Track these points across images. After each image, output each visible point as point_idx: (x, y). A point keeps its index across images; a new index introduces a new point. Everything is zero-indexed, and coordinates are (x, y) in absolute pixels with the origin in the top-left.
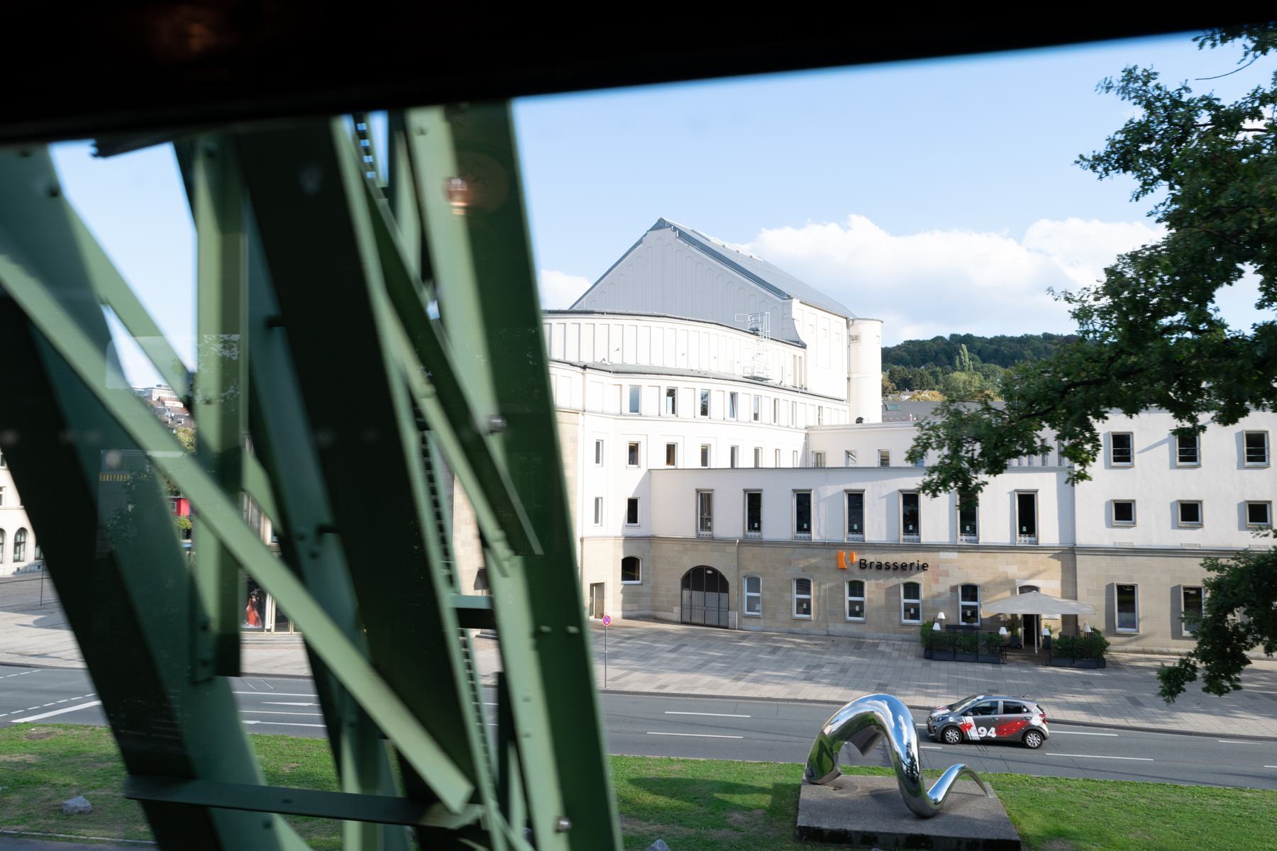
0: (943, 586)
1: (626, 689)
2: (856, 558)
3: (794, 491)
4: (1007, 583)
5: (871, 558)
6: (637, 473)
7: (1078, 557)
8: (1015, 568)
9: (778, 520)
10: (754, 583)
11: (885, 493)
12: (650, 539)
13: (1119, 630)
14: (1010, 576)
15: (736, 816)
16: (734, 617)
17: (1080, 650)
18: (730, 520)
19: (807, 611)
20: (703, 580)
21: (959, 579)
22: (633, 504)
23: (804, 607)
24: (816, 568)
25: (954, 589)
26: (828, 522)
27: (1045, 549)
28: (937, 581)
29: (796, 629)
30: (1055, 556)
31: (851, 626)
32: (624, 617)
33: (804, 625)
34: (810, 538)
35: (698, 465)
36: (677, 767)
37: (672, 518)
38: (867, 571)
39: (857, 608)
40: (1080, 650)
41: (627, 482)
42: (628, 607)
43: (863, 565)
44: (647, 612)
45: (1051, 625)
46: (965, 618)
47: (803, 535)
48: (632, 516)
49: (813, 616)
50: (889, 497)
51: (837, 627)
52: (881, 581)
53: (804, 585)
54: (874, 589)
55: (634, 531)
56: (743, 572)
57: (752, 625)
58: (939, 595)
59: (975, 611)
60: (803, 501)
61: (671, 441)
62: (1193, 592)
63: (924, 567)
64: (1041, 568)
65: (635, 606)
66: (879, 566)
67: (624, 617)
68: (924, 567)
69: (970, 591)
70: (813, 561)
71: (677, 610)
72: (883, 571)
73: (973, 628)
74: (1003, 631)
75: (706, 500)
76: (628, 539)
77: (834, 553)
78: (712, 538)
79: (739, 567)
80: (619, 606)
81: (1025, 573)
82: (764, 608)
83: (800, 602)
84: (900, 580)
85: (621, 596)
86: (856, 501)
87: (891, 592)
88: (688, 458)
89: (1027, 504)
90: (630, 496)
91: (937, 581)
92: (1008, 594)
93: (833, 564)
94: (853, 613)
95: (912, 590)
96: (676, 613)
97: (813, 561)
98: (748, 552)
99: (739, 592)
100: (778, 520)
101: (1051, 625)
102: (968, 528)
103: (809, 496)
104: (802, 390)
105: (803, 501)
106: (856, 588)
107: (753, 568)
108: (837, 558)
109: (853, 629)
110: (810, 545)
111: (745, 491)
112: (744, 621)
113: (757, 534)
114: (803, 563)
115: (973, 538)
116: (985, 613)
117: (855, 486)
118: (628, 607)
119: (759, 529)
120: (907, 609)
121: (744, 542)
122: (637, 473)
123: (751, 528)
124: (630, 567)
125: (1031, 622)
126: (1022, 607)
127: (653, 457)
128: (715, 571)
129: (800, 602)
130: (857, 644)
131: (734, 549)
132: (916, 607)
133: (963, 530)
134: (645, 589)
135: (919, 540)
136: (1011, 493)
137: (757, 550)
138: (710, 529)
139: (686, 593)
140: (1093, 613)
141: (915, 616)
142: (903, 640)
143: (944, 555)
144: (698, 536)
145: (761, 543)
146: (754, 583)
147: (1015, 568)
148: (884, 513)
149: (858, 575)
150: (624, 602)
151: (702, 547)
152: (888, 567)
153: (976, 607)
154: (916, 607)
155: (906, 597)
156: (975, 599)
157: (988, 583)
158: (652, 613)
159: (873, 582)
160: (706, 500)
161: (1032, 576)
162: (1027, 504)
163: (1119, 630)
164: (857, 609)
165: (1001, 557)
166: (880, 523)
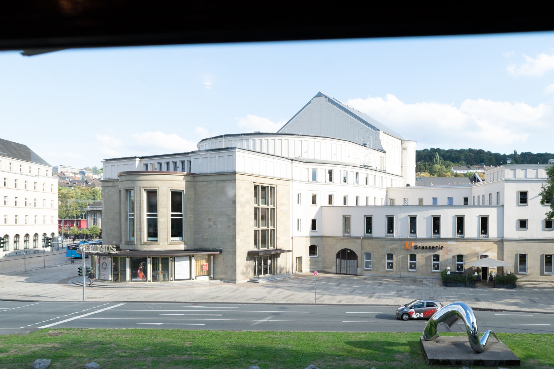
0: (449, 256)
1: (325, 303)
2: (413, 244)
3: (387, 216)
4: (476, 254)
5: (419, 244)
6: (315, 208)
8: (479, 248)
9: (380, 228)
10: (369, 256)
11: (426, 217)
12: (322, 237)
13: (519, 272)
14: (477, 251)
15: (398, 356)
16: (360, 270)
17: (506, 281)
18: (358, 228)
19: (392, 267)
20: (346, 255)
22: (314, 222)
23: (390, 266)
24: (396, 249)
25: (454, 257)
26: (401, 229)
28: (447, 254)
29: (386, 275)
30: (495, 243)
31: (411, 273)
32: (311, 272)
33: (390, 273)
34: (393, 236)
35: (342, 204)
36: (363, 336)
37: (332, 228)
38: (417, 250)
39: (413, 266)
40: (506, 281)
41: (312, 212)
42: (312, 267)
43: (416, 247)
44: (321, 269)
45: (493, 271)
46: (458, 269)
47: (390, 235)
48: (314, 227)
49: (394, 269)
50: (427, 218)
52: (424, 254)
53: (390, 256)
54: (420, 258)
55: (315, 233)
56: (364, 251)
57: (368, 274)
58: (448, 260)
59: (462, 266)
60: (391, 220)
61: (331, 194)
62: (549, 257)
63: (442, 248)
64: (490, 248)
65: (315, 267)
66: (423, 248)
67: (311, 272)
68: (442, 248)
69: (460, 258)
70: (394, 246)
71: (334, 268)
72: (424, 250)
73: (461, 273)
74: (476, 274)
76: (312, 237)
77: (403, 242)
78: (350, 237)
79: (362, 249)
80: (309, 267)
81: (483, 250)
82: (373, 267)
83: (389, 264)
85: (309, 263)
86: (413, 220)
87: (428, 259)
88: (338, 201)
89: (484, 221)
90: (313, 218)
91: (447, 254)
92: (476, 259)
93: (403, 247)
94: (411, 268)
95: (437, 258)
96: (334, 269)
97: (394, 246)
98: (366, 242)
99: (362, 260)
100: (380, 228)
101: (493, 271)
102: (460, 231)
103: (393, 218)
104: (384, 172)
105: (391, 220)
106: (413, 257)
107: (368, 249)
108: (405, 245)
109: (412, 275)
110: (394, 239)
111: (365, 216)
112: (364, 272)
113: (370, 234)
114: (390, 247)
115: (462, 235)
116: (466, 267)
117: (413, 214)
118: (312, 267)
119: (371, 232)
120: (434, 266)
121: (364, 238)
122: (315, 208)
123: (367, 232)
124: (313, 250)
125: (485, 270)
126: (482, 264)
127: (323, 201)
128: (351, 251)
129: (389, 264)
130: (414, 281)
131: (360, 241)
132: (438, 265)
133: (458, 232)
134: (320, 259)
135: (440, 237)
136: (478, 217)
137: (370, 241)
138: (349, 232)
139: (338, 260)
140: (509, 266)
141: (438, 268)
142: (432, 279)
143: (450, 243)
144: (344, 236)
145: (372, 238)
146: (369, 256)
147: (479, 248)
148: (425, 225)
149: (413, 252)
150: (311, 265)
151: (346, 240)
152: (426, 248)
153: (462, 264)
154: (438, 265)
155: (458, 261)
156: (462, 261)
157: (467, 255)
158: (323, 269)
159: (420, 254)
160: (347, 220)
161: (486, 251)
162: (484, 221)
163: (519, 272)
164: (413, 266)
165: (474, 243)
166: (424, 229)
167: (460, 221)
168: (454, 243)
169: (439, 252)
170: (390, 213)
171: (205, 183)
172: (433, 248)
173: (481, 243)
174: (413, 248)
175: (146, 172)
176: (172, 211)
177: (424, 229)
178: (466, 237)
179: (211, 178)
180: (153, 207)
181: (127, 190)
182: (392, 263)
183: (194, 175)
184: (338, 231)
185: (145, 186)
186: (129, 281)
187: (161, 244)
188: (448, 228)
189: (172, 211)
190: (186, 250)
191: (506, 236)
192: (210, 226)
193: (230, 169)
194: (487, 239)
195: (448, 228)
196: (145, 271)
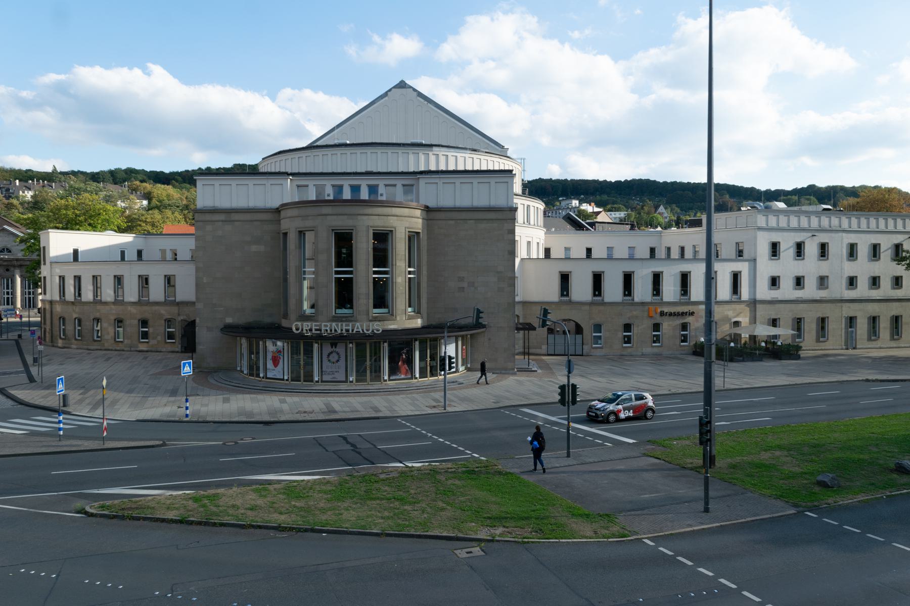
2: (659, 310)
5: (666, 310)
7: (758, 306)
18: (581, 290)
23: (628, 340)
26: (642, 290)
27: (744, 302)
29: (624, 353)
30: (748, 306)
43: (662, 314)
51: (648, 350)
53: (627, 327)
54: (668, 326)
57: (598, 353)
66: (671, 314)
70: (635, 313)
71: (544, 347)
75: (565, 278)
77: (646, 308)
78: (570, 302)
84: (679, 321)
93: (646, 314)
94: (654, 342)
95: (684, 327)
97: (635, 313)
100: (613, 290)
106: (657, 327)
109: (656, 350)
121: (591, 304)
129: (625, 336)
145: (603, 303)
149: (658, 319)
160: (565, 278)
164: (657, 339)
165: (727, 307)
167: (657, 278)
169: (689, 319)
170: (628, 269)
171: (452, 222)
172: (683, 314)
173: (733, 306)
174: (658, 315)
175: (373, 202)
176: (337, 266)
177: (670, 290)
178: (692, 300)
179: (464, 215)
180: (381, 257)
181: (300, 232)
182: (629, 337)
183: (427, 209)
184: (552, 293)
185: (376, 224)
186: (317, 382)
187: (398, 318)
189: (337, 266)
190: (423, 327)
191: (760, 296)
192: (462, 289)
193: (500, 202)
194: (740, 301)
196: (410, 362)
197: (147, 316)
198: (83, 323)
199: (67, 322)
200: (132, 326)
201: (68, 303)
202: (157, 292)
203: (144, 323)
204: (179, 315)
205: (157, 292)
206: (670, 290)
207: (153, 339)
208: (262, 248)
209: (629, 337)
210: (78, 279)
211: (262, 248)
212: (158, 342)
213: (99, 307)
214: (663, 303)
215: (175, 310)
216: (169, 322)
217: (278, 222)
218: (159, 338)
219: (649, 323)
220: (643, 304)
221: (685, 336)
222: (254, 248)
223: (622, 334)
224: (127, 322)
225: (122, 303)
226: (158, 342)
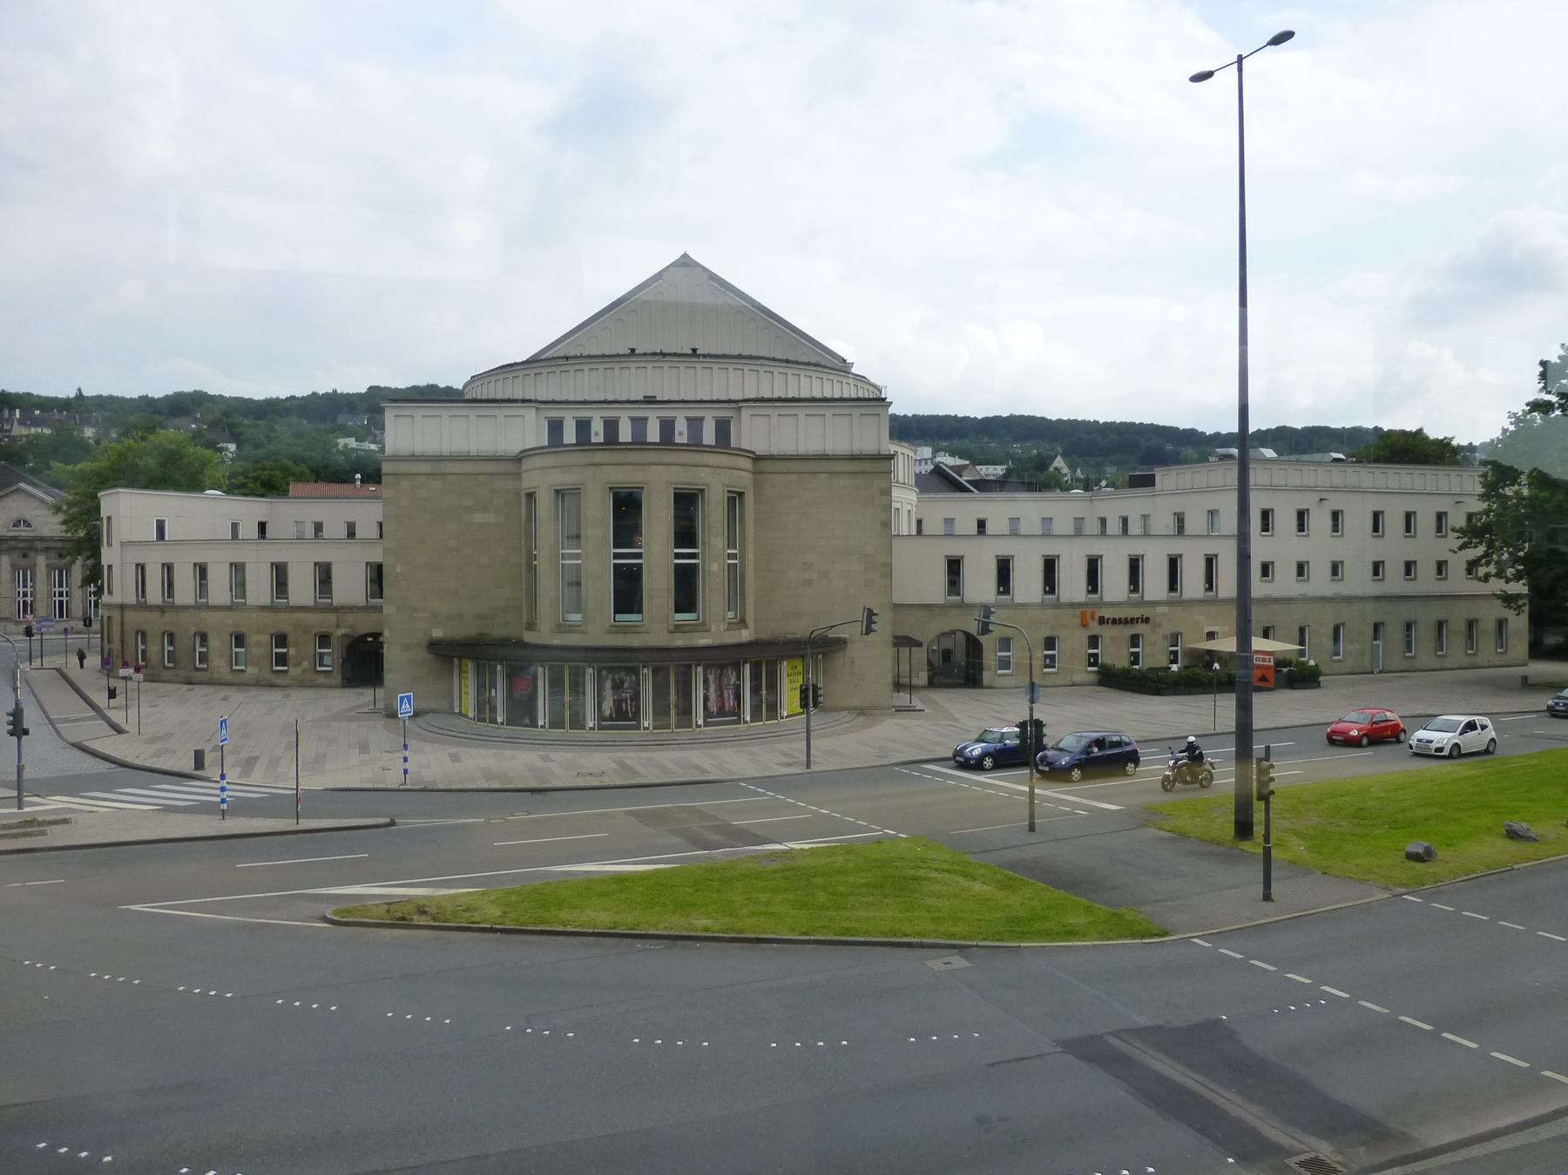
5: (1107, 613)
21: (1168, 629)
25: (1165, 637)
43: (1102, 621)
53: (1050, 643)
57: (1006, 682)
63: (1147, 620)
66: (1114, 621)
68: (1147, 620)
75: (954, 566)
106: (1094, 641)
129: (1046, 656)
143: (1160, 609)
149: (1095, 628)
160: (954, 566)
168: (1165, 609)
169: (1140, 628)
172: (1133, 621)
177: (1115, 584)
181: (557, 492)
182: (1052, 658)
184: (933, 588)
188: (1155, 582)
195: (1155, 582)
197: (285, 628)
198: (177, 640)
199: (149, 638)
200: (259, 642)
201: (151, 608)
202: (302, 589)
203: (281, 640)
204: (338, 626)
205: (302, 589)
206: (1115, 584)
207: (297, 665)
208: (491, 518)
209: (1052, 658)
210: (168, 568)
211: (491, 518)
212: (304, 670)
213: (204, 614)
214: (1101, 604)
215: (331, 618)
216: (324, 640)
217: (518, 476)
218: (305, 664)
219: (1082, 637)
220: (1073, 605)
221: (1136, 655)
222: (478, 518)
223: (1040, 653)
224: (252, 638)
225: (243, 608)
226: (304, 670)
